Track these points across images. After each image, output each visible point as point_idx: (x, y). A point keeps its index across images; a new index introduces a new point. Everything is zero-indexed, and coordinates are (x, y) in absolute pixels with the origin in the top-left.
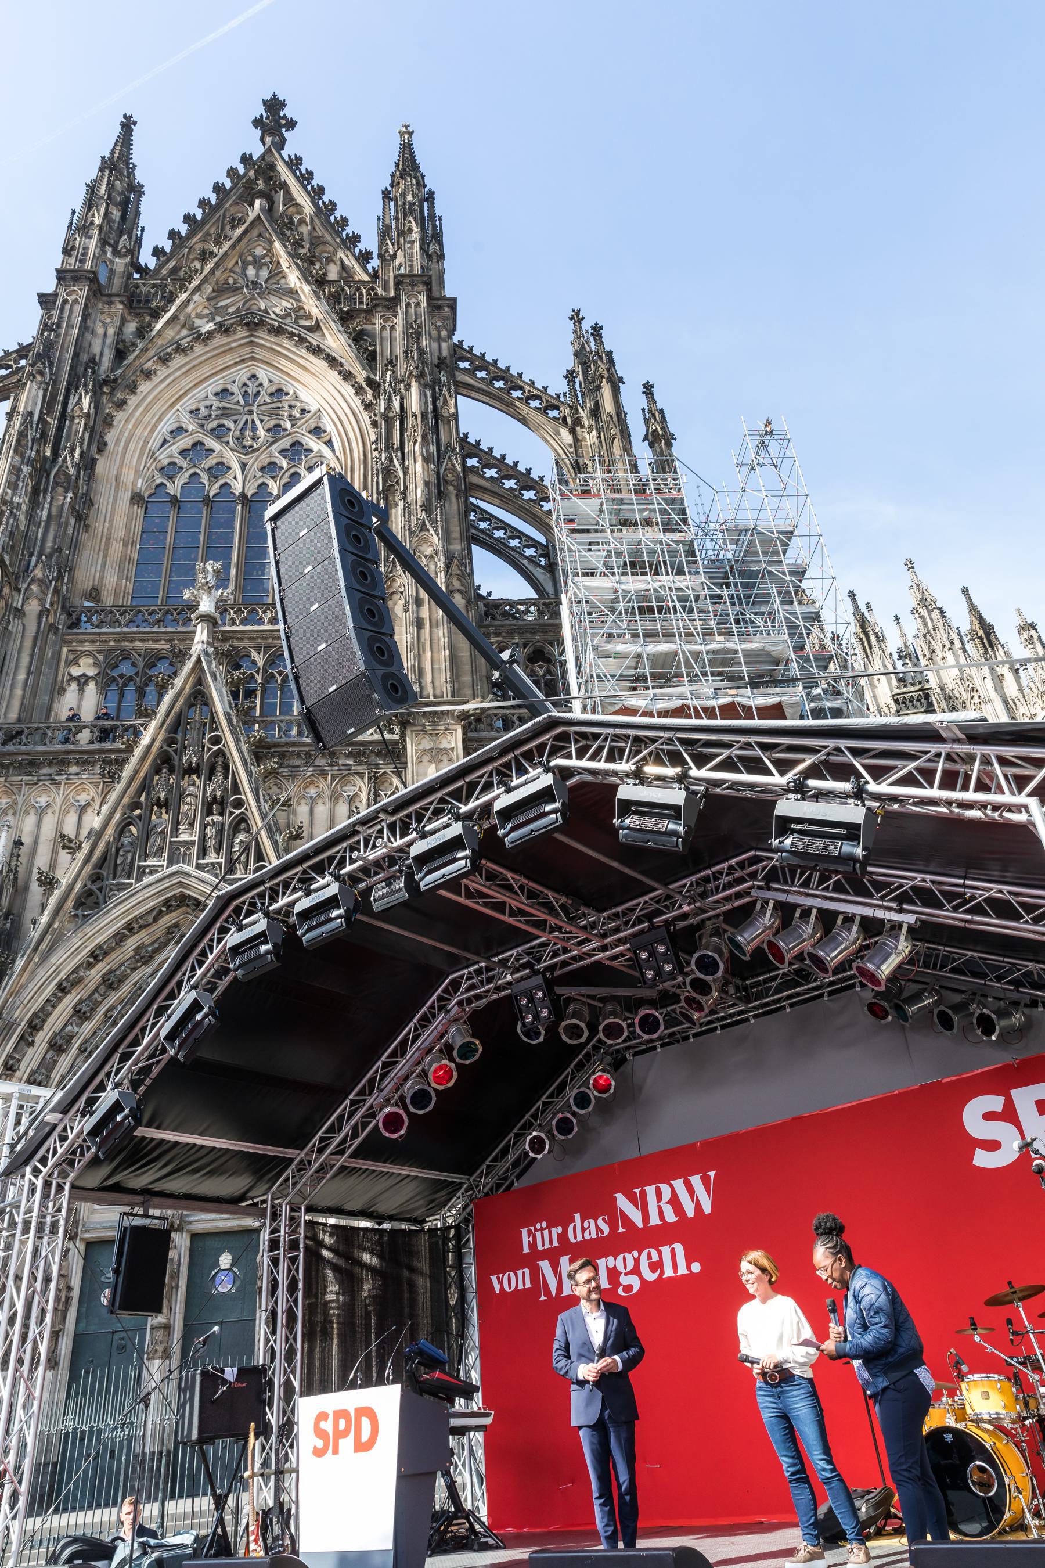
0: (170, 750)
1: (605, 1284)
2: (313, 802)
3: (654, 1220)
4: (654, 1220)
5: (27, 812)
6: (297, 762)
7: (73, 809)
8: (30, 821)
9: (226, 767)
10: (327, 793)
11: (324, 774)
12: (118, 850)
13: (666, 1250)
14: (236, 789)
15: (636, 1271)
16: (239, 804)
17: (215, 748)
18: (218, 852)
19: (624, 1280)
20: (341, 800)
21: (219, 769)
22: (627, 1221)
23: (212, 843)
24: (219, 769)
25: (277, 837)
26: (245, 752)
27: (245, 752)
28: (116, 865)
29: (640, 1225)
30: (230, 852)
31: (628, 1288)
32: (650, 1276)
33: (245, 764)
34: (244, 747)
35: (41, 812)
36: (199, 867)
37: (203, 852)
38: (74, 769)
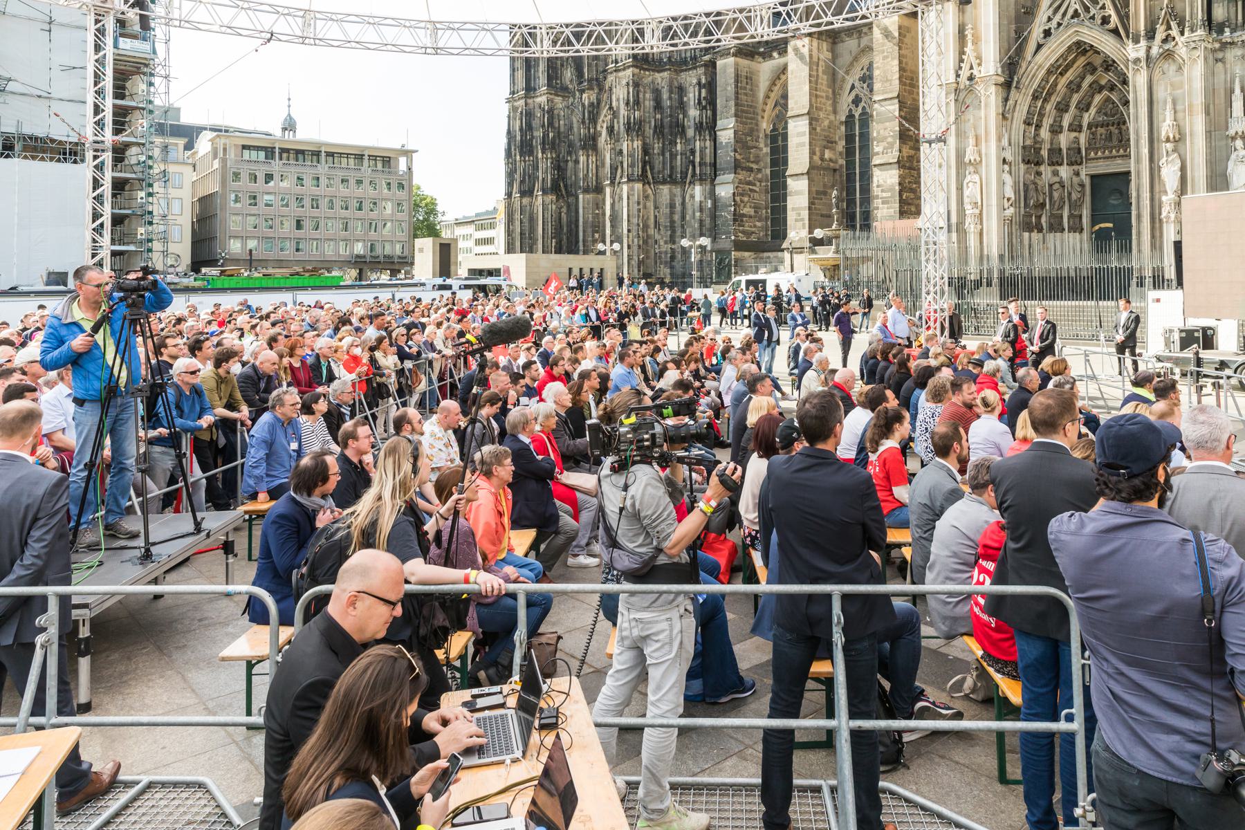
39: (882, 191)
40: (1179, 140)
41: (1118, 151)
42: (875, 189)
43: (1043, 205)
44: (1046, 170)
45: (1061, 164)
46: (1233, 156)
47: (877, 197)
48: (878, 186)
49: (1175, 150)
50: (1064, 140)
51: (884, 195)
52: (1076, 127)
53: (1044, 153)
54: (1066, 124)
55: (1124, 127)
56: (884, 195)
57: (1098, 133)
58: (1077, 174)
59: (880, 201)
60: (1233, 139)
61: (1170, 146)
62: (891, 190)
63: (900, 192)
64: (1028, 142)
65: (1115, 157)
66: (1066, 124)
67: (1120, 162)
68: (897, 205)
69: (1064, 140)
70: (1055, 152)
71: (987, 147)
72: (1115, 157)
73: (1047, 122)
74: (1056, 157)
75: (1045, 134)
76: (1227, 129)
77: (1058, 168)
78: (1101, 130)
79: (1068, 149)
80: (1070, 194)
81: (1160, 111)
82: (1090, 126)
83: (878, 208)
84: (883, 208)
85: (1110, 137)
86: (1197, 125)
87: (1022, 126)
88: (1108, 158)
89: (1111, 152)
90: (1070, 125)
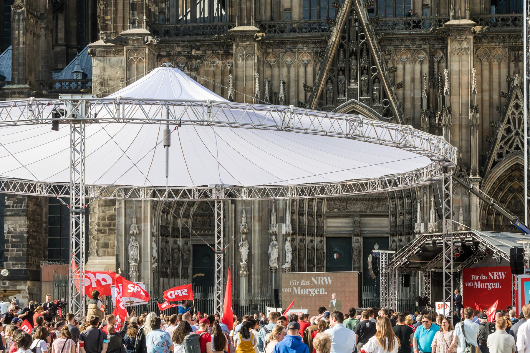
0: (343, 42)
1: (486, 287)
2: (404, 63)
3: (495, 278)
4: (495, 278)
5: (283, 66)
6: (397, 43)
7: (302, 65)
8: (285, 70)
9: (368, 51)
10: (411, 59)
11: (409, 48)
12: (326, 91)
13: (496, 283)
14: (373, 63)
15: (491, 286)
16: (375, 70)
17: (363, 41)
18: (368, 93)
19: (489, 287)
20: (417, 63)
21: (365, 51)
22: (490, 277)
23: (365, 89)
24: (365, 51)
25: (392, 88)
26: (376, 44)
27: (376, 44)
28: (327, 98)
29: (492, 278)
30: (372, 93)
31: (489, 288)
32: (493, 287)
33: (377, 52)
34: (375, 42)
35: (289, 66)
36: (361, 100)
37: (361, 95)
38: (300, 46)
39: (12, 237)
40: (249, 233)
41: (208, 232)
42: (5, 235)
43: (169, 261)
44: (171, 240)
45: (178, 237)
46: (271, 244)
47: (8, 241)
48: (8, 233)
49: (246, 239)
50: (180, 222)
51: (14, 240)
52: (186, 216)
53: (170, 229)
54: (181, 213)
55: (212, 218)
56: (14, 240)
57: (198, 220)
58: (186, 243)
59: (10, 244)
60: (271, 235)
61: (244, 236)
62: (20, 236)
63: (28, 238)
64: (164, 224)
65: (207, 235)
66: (181, 213)
67: (209, 238)
68: (25, 249)
69: (180, 222)
70: (175, 229)
71: (144, 225)
72: (207, 235)
73: (172, 212)
74: (176, 233)
75: (170, 218)
76: (268, 229)
77: (177, 239)
78: (199, 219)
79: (182, 228)
80: (183, 255)
81: (239, 217)
82: (193, 217)
83: (8, 250)
84: (12, 251)
85: (204, 223)
86: (257, 226)
87: (161, 213)
88: (203, 235)
89: (201, 232)
90: (184, 214)
